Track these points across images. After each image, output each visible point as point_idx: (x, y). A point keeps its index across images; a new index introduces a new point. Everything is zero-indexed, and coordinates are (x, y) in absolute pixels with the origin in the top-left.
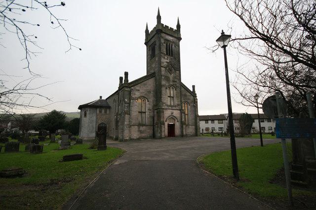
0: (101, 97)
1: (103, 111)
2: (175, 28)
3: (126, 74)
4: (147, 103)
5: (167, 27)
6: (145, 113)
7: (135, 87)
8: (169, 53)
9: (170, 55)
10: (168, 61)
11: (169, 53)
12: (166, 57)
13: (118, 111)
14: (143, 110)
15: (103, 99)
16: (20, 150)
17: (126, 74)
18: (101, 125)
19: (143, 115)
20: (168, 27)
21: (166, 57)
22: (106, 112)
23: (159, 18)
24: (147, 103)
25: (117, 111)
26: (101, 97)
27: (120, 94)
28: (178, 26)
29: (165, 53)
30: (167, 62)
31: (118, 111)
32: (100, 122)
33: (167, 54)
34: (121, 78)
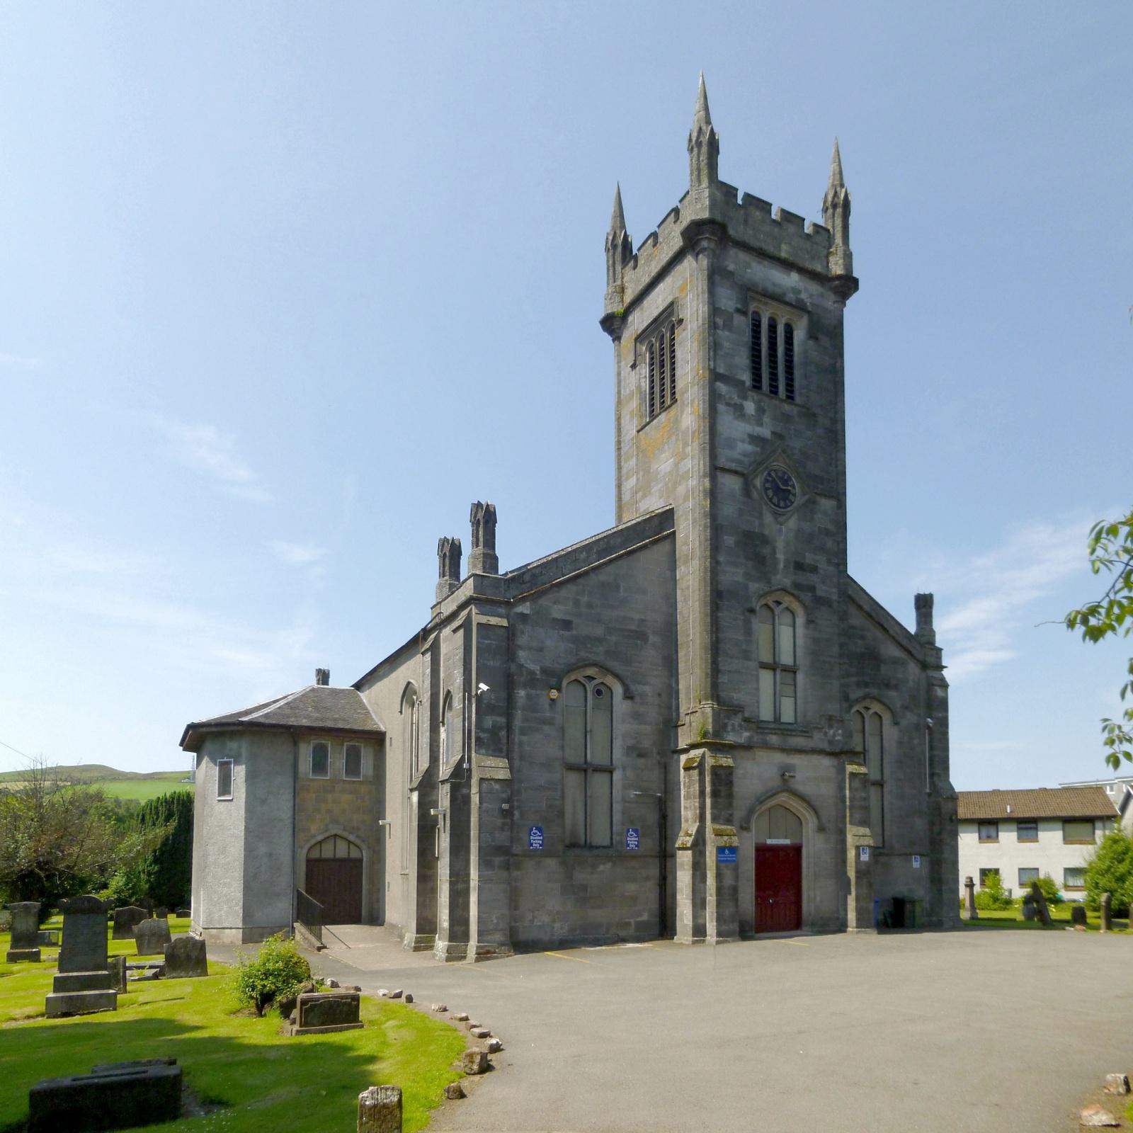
0: (323, 676)
1: (337, 761)
2: (813, 215)
3: (485, 519)
4: (621, 706)
5: (757, 204)
6: (610, 771)
7: (544, 601)
8: (774, 377)
9: (774, 390)
10: (766, 432)
11: (774, 377)
12: (750, 407)
13: (434, 758)
14: (597, 755)
15: (334, 683)
16: (209, 971)
17: (485, 519)
18: (327, 852)
19: (599, 781)
20: (765, 206)
21: (750, 407)
22: (320, 765)
23: (707, 148)
24: (621, 706)
25: (424, 764)
26: (323, 676)
27: (444, 648)
28: (841, 206)
29: (746, 377)
30: (754, 439)
31: (434, 758)
32: (316, 830)
33: (757, 385)
34: (450, 553)
